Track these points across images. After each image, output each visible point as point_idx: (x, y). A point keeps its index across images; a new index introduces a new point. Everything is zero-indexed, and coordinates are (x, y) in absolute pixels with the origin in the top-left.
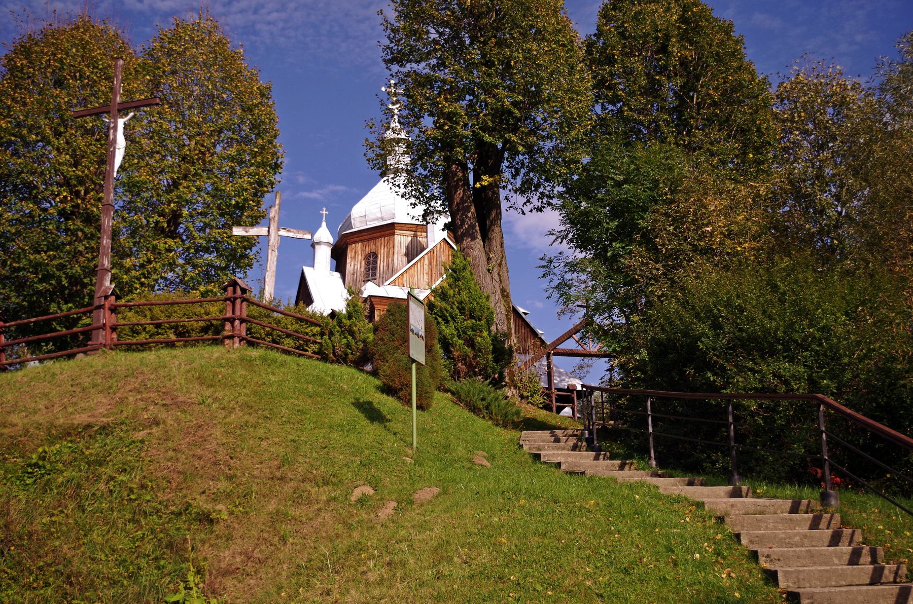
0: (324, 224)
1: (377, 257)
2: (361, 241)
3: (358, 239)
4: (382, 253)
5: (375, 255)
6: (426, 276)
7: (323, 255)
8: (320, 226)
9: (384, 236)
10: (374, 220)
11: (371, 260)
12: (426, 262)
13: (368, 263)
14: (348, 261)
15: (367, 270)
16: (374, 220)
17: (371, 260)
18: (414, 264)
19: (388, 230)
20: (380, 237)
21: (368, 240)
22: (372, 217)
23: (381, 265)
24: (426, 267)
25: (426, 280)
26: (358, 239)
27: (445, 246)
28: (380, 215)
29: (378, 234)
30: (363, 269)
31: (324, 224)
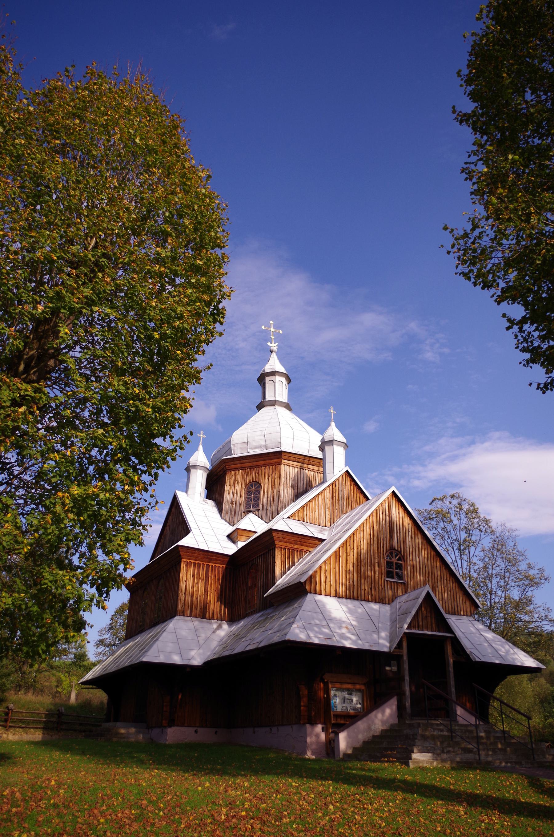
2: (242, 468)
3: (238, 466)
5: (257, 484)
6: (327, 512)
7: (199, 479)
10: (256, 447)
11: (253, 491)
12: (328, 495)
14: (227, 488)
16: (256, 447)
20: (265, 465)
21: (250, 468)
22: (255, 444)
23: (265, 495)
24: (327, 501)
25: (328, 516)
26: (238, 466)
27: (347, 479)
28: (263, 443)
29: (262, 463)
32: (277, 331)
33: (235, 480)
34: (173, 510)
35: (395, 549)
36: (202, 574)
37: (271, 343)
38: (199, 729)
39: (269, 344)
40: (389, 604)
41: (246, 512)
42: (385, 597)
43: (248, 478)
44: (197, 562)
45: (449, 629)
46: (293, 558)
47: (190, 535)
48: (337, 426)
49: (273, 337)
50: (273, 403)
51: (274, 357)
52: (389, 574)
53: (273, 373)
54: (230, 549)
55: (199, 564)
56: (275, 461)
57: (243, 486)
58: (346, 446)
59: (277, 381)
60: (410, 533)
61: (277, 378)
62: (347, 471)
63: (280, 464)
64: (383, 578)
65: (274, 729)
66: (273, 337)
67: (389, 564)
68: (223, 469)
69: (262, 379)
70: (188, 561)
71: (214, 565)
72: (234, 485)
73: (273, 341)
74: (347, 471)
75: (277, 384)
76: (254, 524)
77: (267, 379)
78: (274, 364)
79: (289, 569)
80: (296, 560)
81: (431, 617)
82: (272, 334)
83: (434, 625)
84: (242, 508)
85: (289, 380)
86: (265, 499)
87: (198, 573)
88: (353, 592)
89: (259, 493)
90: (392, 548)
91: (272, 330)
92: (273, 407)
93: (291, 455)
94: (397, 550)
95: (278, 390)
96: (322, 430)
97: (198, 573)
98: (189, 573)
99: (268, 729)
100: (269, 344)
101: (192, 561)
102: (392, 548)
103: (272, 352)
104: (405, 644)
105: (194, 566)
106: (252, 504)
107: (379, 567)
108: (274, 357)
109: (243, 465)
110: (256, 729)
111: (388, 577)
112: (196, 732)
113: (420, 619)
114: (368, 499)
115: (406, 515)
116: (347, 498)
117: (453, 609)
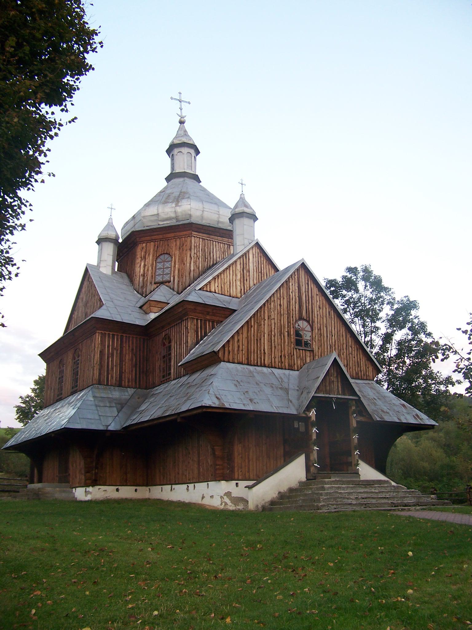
26: (148, 238)
27: (256, 250)
29: (172, 235)
33: (146, 252)
34: (86, 283)
38: (119, 487)
40: (298, 370)
42: (294, 364)
45: (354, 393)
47: (104, 307)
55: (113, 335)
56: (185, 233)
60: (318, 303)
63: (190, 236)
64: (292, 346)
65: (191, 486)
71: (128, 336)
72: (145, 258)
76: (165, 296)
81: (338, 382)
88: (264, 360)
99: (185, 486)
109: (154, 237)
110: (174, 486)
111: (296, 345)
112: (117, 490)
117: (357, 374)
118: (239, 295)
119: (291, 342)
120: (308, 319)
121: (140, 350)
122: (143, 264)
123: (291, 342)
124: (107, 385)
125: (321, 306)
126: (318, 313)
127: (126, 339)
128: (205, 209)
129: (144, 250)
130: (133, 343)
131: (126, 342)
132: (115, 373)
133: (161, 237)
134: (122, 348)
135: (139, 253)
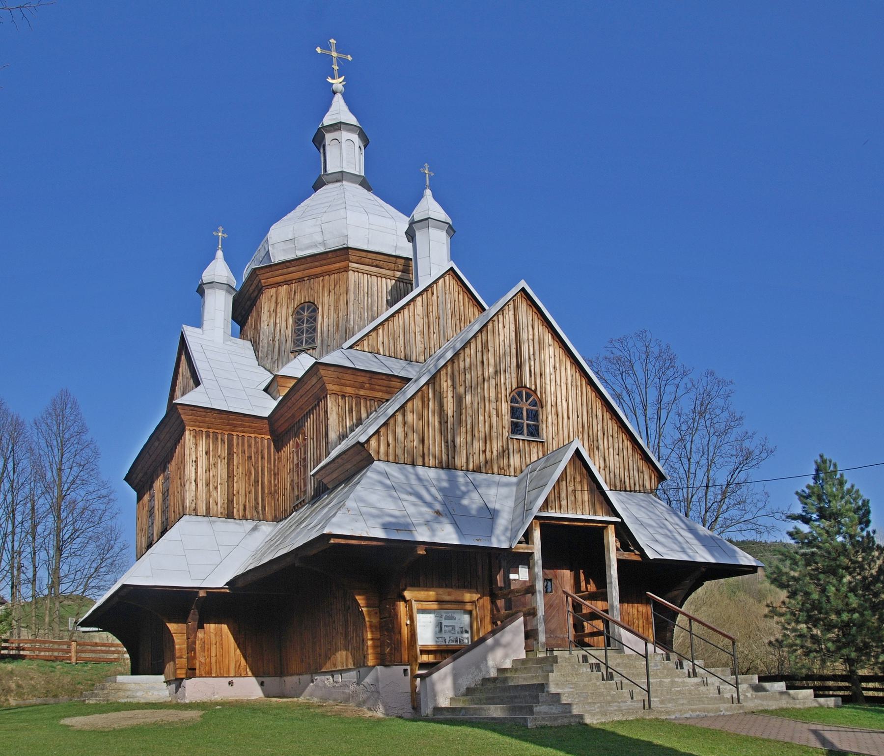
0: (220, 254)
1: (315, 310)
2: (287, 282)
4: (325, 302)
5: (312, 307)
6: (419, 338)
7: (218, 306)
8: (213, 257)
9: (329, 273)
11: (306, 314)
13: (298, 321)
14: (265, 317)
15: (298, 332)
16: (308, 248)
17: (306, 314)
18: (398, 312)
19: (339, 259)
20: (322, 274)
21: (300, 280)
22: (307, 241)
23: (325, 321)
30: (289, 332)
31: (220, 254)
32: (342, 56)
33: (276, 303)
35: (525, 387)
36: (223, 451)
37: (333, 78)
39: (330, 80)
41: (296, 352)
43: (298, 297)
44: (211, 431)
46: (359, 412)
48: (436, 197)
49: (336, 68)
50: (341, 177)
51: (338, 102)
52: (516, 428)
53: (337, 126)
54: (266, 406)
56: (338, 265)
57: (291, 311)
58: (451, 230)
59: (343, 140)
60: (552, 360)
61: (345, 135)
62: (452, 269)
63: (346, 269)
64: (506, 434)
66: (336, 68)
67: (515, 412)
68: (257, 286)
69: (319, 141)
70: (197, 429)
71: (241, 434)
72: (275, 311)
73: (336, 74)
74: (452, 269)
75: (344, 145)
77: (328, 137)
78: (339, 111)
79: (352, 430)
80: (364, 415)
82: (335, 61)
83: (587, 504)
84: (289, 345)
85: (363, 136)
86: (325, 329)
87: (216, 449)
89: (315, 320)
90: (521, 385)
91: (334, 54)
92: (339, 184)
93: (364, 254)
94: (530, 389)
95: (345, 154)
96: (407, 210)
97: (216, 449)
98: (200, 449)
100: (330, 80)
101: (204, 430)
102: (521, 385)
103: (335, 93)
104: (537, 535)
105: (208, 436)
106: (305, 335)
107: (497, 416)
108: (338, 102)
111: (513, 432)
113: (563, 495)
114: (484, 309)
115: (546, 330)
116: (453, 314)
118: (422, 359)
119: (503, 427)
120: (533, 388)
121: (263, 458)
122: (272, 321)
123: (503, 427)
124: (208, 514)
125: (557, 365)
126: (553, 377)
127: (238, 439)
128: (371, 227)
129: (274, 299)
130: (250, 446)
131: (238, 444)
132: (220, 496)
133: (299, 275)
134: (230, 454)
135: (266, 303)
